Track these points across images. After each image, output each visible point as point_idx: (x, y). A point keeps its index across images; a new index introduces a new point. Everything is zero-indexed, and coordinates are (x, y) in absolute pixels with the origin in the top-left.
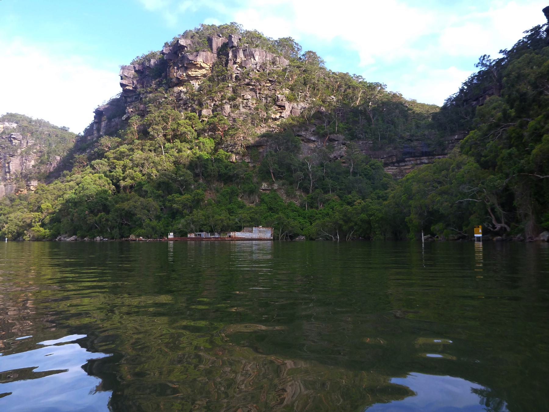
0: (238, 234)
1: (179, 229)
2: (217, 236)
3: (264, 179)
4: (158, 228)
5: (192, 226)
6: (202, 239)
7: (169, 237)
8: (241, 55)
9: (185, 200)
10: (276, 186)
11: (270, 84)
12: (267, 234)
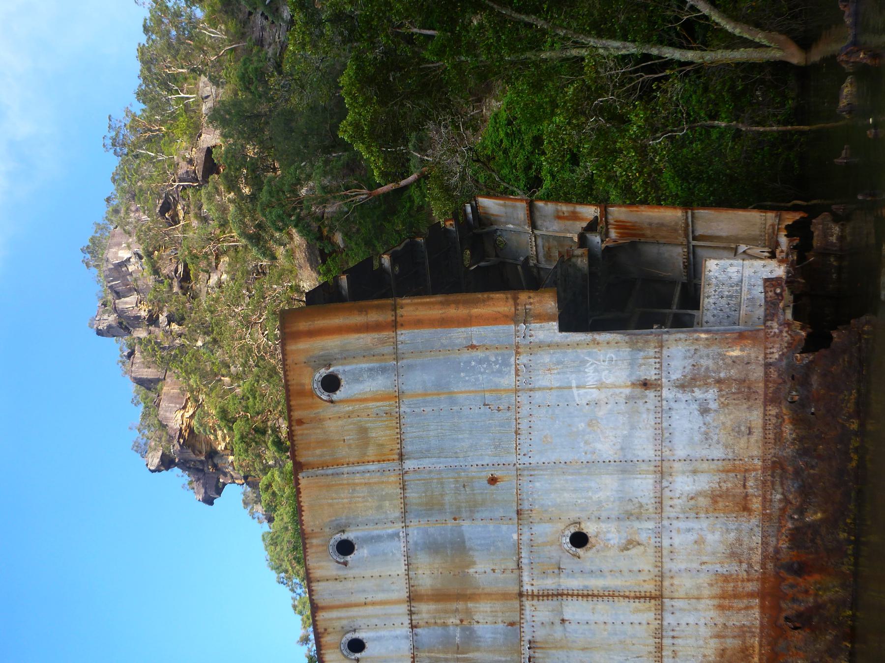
8: (129, 303)
11: (179, 207)
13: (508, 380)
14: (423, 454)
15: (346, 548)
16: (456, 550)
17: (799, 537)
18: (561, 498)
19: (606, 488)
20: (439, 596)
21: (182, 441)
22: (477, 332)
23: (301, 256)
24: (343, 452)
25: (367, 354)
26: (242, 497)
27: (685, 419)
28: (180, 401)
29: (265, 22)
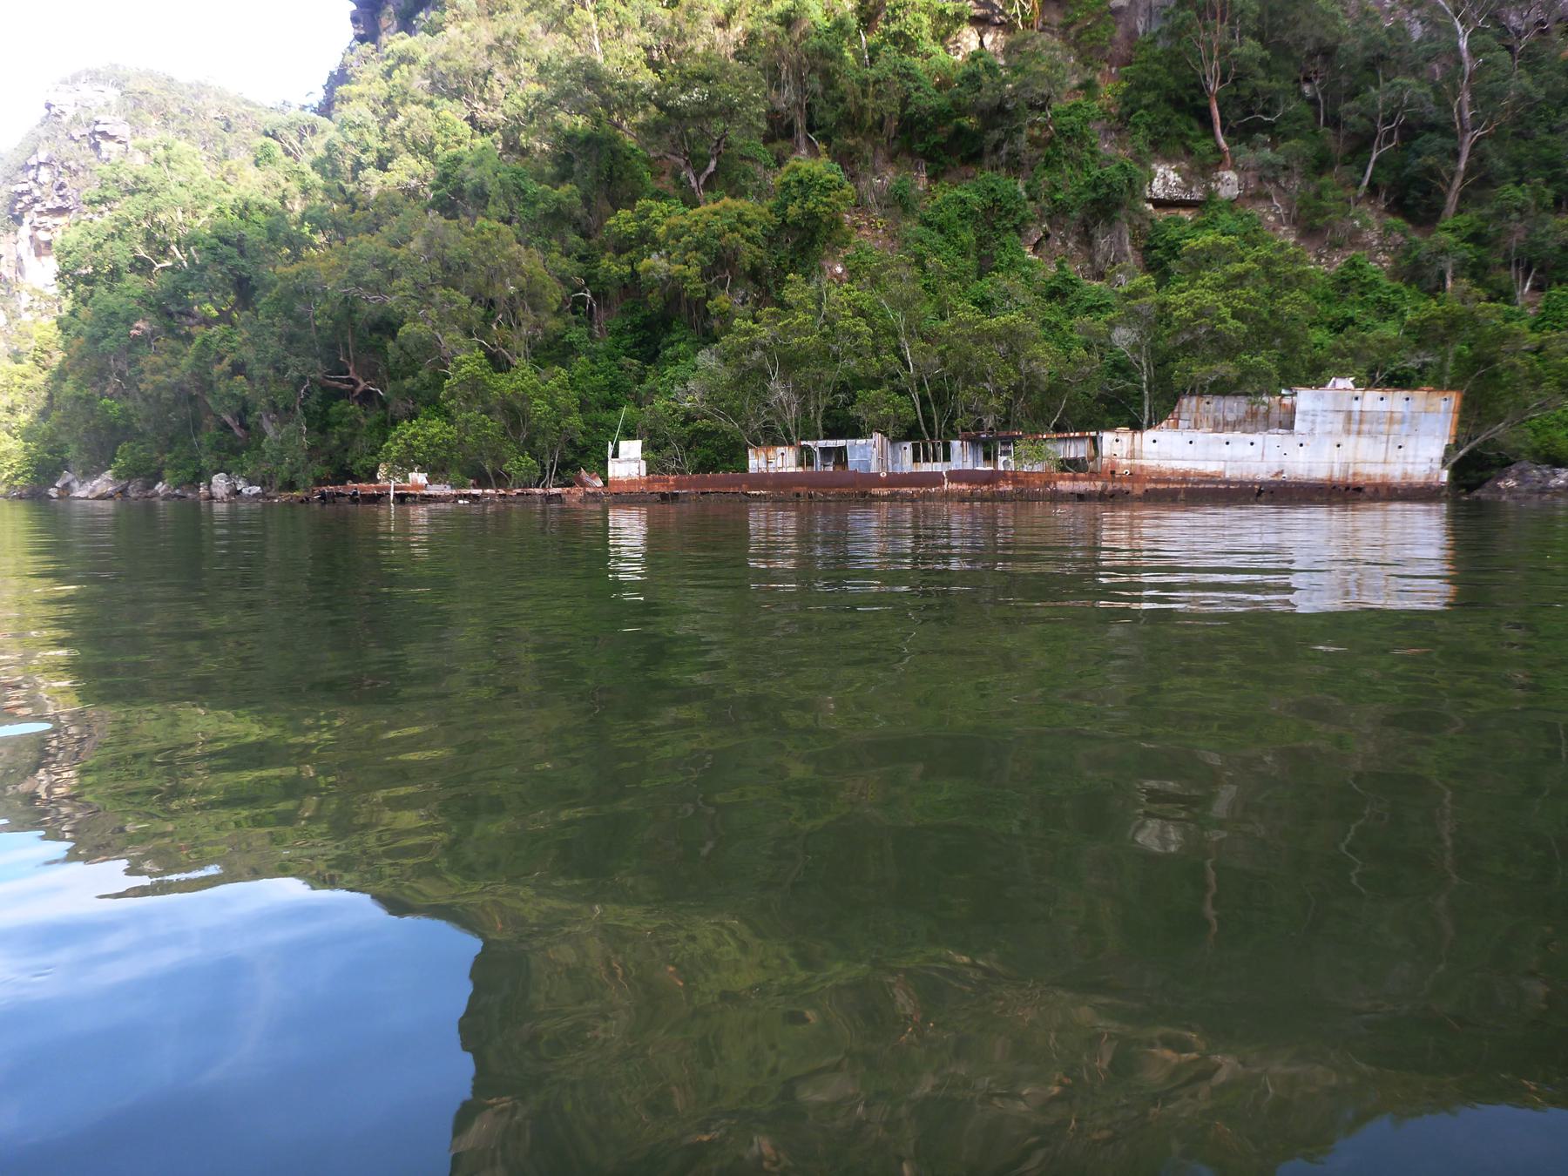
0: (1168, 448)
1: (689, 418)
2: (962, 458)
3: (1161, 146)
4: (540, 407)
5: (778, 390)
6: (862, 490)
7: (617, 470)
9: (719, 225)
10: (1229, 183)
12: (1415, 437)
16: (1402, 421)
18: (1410, 444)
19: (1411, 452)
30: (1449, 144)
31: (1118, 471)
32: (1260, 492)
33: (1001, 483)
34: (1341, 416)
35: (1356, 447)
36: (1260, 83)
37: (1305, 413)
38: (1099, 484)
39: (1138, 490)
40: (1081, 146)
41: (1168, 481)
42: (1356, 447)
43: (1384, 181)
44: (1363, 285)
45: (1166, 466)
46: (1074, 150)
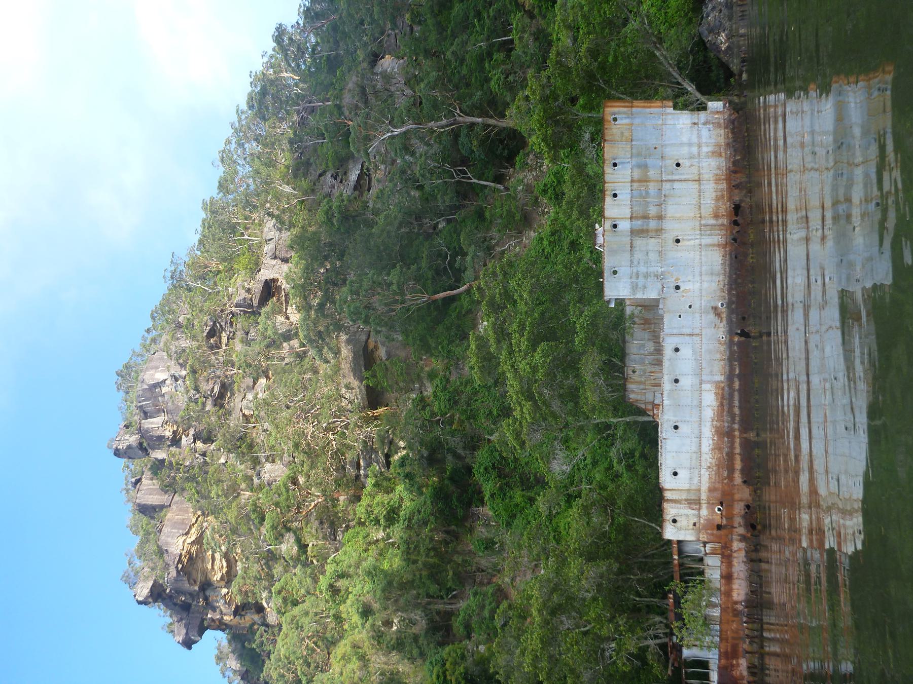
0: (689, 459)
8: (155, 424)
11: (223, 334)
13: (660, 122)
14: (637, 141)
15: (615, 165)
16: (644, 167)
17: (735, 163)
18: (673, 153)
19: (685, 150)
20: (639, 181)
21: (180, 566)
22: (652, 110)
23: (346, 366)
24: (617, 138)
25: (624, 113)
26: (216, 652)
27: (705, 132)
28: (183, 527)
29: (334, 181)
30: (464, 132)
31: (718, 520)
32: (743, 334)
33: (736, 673)
34: (639, 242)
35: (679, 219)
36: (423, 265)
37: (635, 287)
38: (736, 545)
39: (744, 494)
40: (462, 392)
41: (730, 456)
42: (679, 219)
43: (491, 172)
44: (559, 182)
45: (708, 457)
46: (464, 398)
